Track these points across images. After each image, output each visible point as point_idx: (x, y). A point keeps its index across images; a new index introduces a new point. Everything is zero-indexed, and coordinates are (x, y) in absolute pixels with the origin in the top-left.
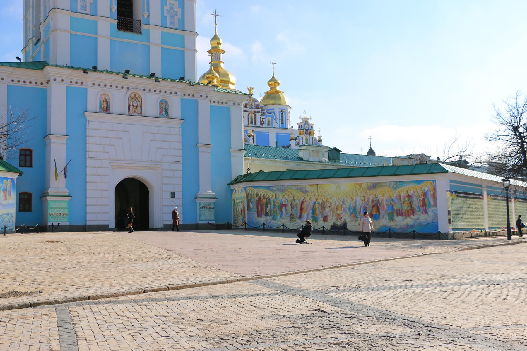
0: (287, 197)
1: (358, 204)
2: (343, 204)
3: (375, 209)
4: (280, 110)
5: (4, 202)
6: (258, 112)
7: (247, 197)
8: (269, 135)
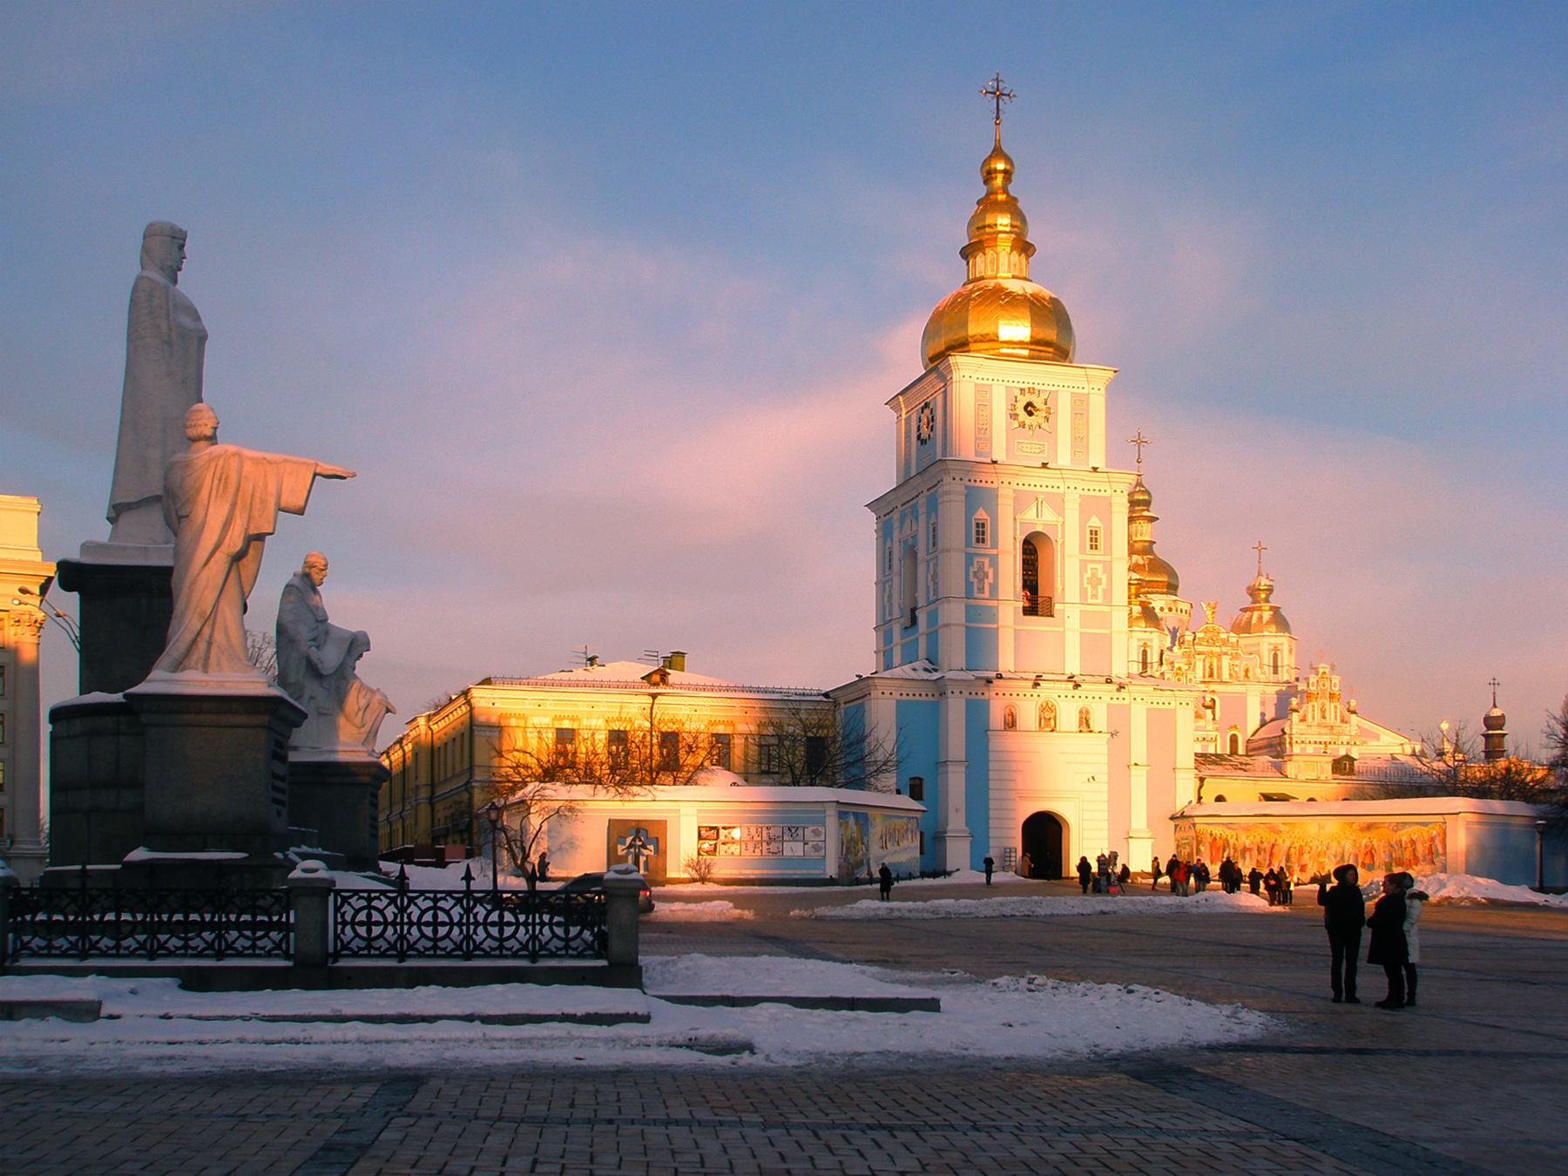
0: (1251, 837)
1: (1346, 849)
2: (1328, 848)
3: (1368, 856)
4: (1272, 647)
5: (912, 845)
6: (1226, 654)
7: (1197, 836)
8: (1246, 698)
